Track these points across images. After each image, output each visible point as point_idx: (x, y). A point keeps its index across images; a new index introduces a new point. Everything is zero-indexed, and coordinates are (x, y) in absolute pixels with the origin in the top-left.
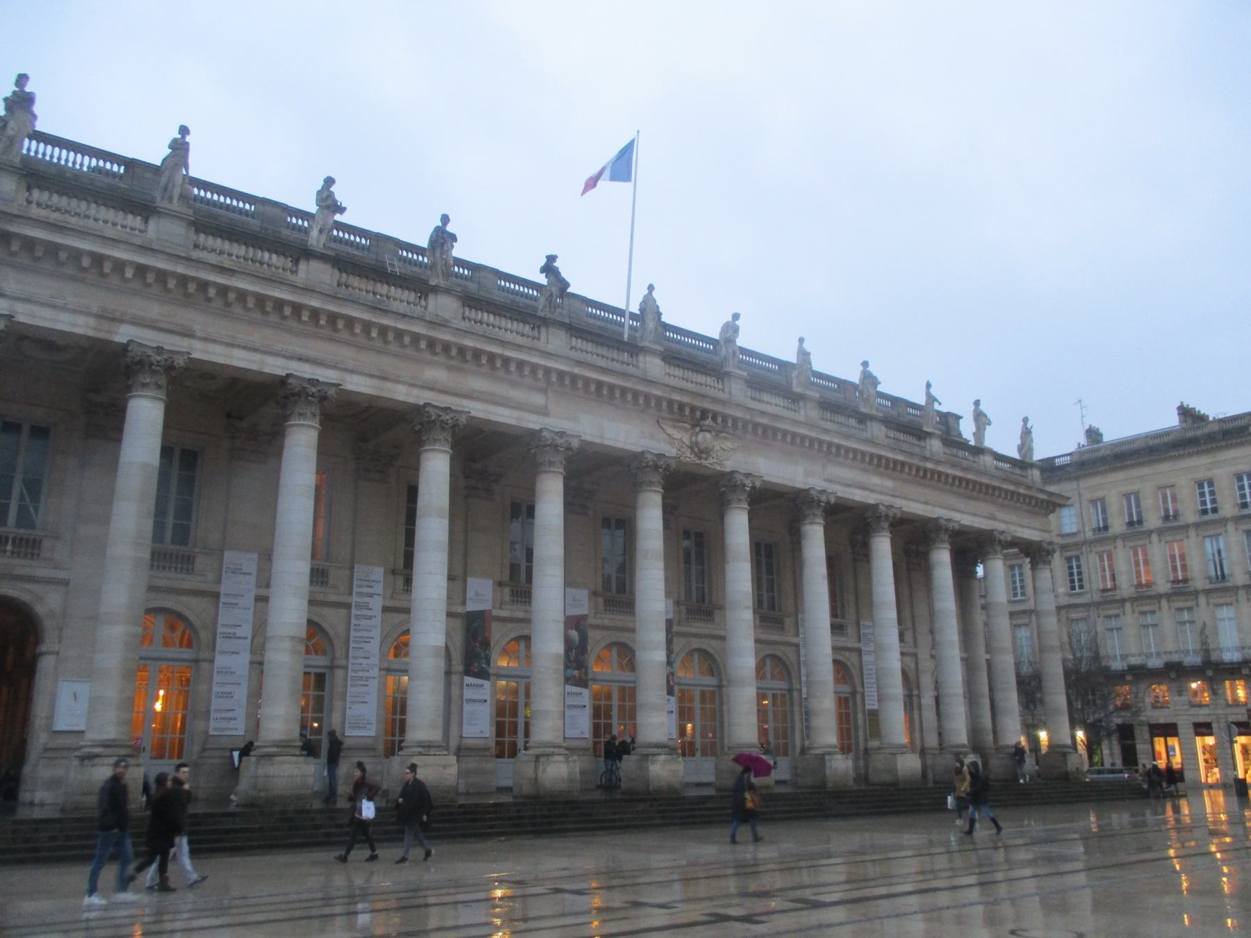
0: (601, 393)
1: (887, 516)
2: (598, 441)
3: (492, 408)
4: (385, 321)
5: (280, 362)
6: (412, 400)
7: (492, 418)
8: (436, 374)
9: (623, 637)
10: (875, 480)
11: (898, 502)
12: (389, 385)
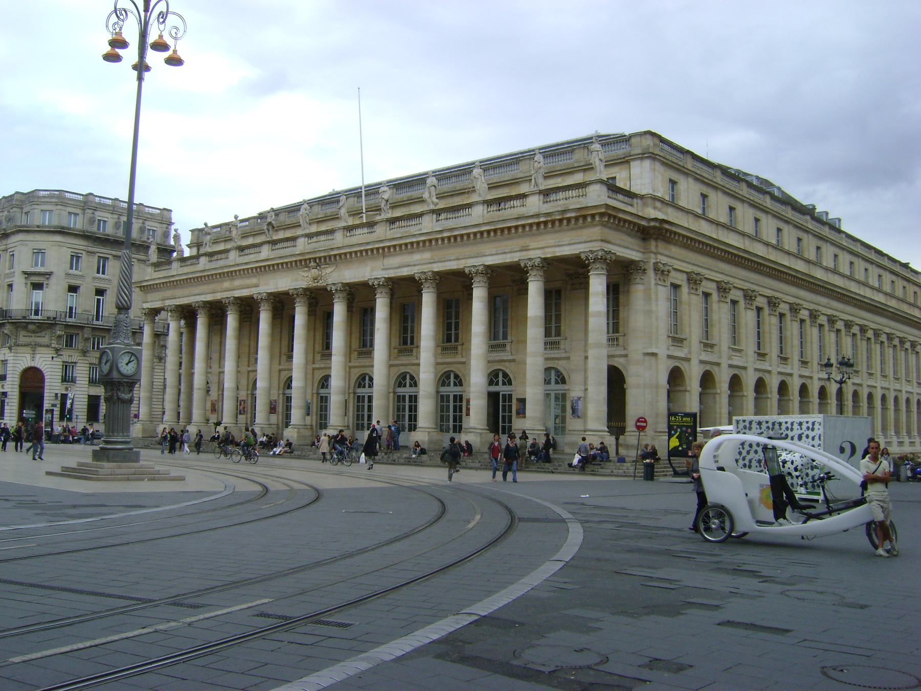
9: (367, 371)
10: (417, 257)
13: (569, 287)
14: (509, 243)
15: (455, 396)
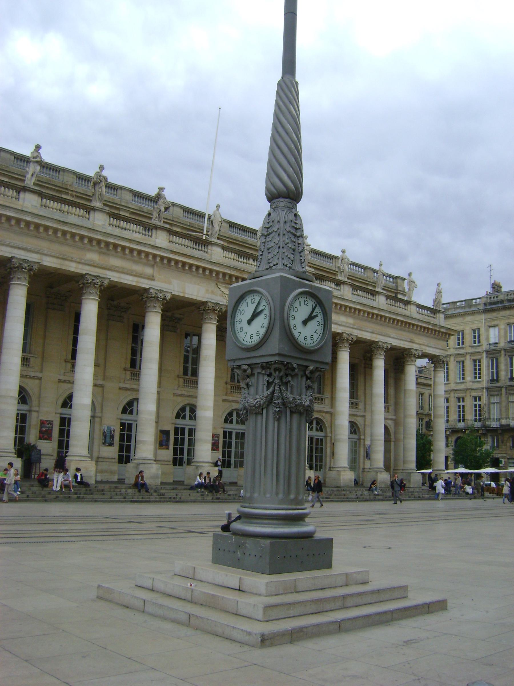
0: (185, 268)
1: (348, 340)
2: (181, 295)
3: (123, 276)
4: (65, 228)
5: (9, 249)
6: (79, 271)
7: (122, 281)
8: (93, 256)
11: (356, 332)
12: (67, 263)
13: (363, 365)
14: (404, 333)
15: (237, 434)
